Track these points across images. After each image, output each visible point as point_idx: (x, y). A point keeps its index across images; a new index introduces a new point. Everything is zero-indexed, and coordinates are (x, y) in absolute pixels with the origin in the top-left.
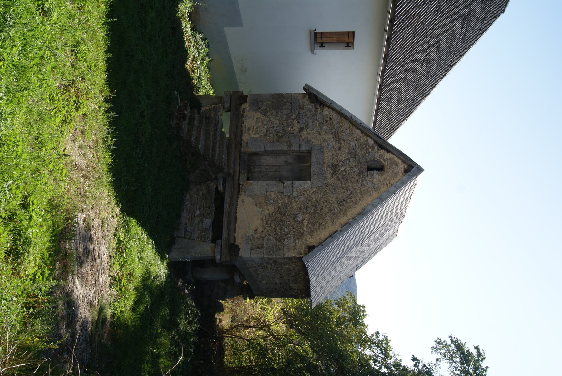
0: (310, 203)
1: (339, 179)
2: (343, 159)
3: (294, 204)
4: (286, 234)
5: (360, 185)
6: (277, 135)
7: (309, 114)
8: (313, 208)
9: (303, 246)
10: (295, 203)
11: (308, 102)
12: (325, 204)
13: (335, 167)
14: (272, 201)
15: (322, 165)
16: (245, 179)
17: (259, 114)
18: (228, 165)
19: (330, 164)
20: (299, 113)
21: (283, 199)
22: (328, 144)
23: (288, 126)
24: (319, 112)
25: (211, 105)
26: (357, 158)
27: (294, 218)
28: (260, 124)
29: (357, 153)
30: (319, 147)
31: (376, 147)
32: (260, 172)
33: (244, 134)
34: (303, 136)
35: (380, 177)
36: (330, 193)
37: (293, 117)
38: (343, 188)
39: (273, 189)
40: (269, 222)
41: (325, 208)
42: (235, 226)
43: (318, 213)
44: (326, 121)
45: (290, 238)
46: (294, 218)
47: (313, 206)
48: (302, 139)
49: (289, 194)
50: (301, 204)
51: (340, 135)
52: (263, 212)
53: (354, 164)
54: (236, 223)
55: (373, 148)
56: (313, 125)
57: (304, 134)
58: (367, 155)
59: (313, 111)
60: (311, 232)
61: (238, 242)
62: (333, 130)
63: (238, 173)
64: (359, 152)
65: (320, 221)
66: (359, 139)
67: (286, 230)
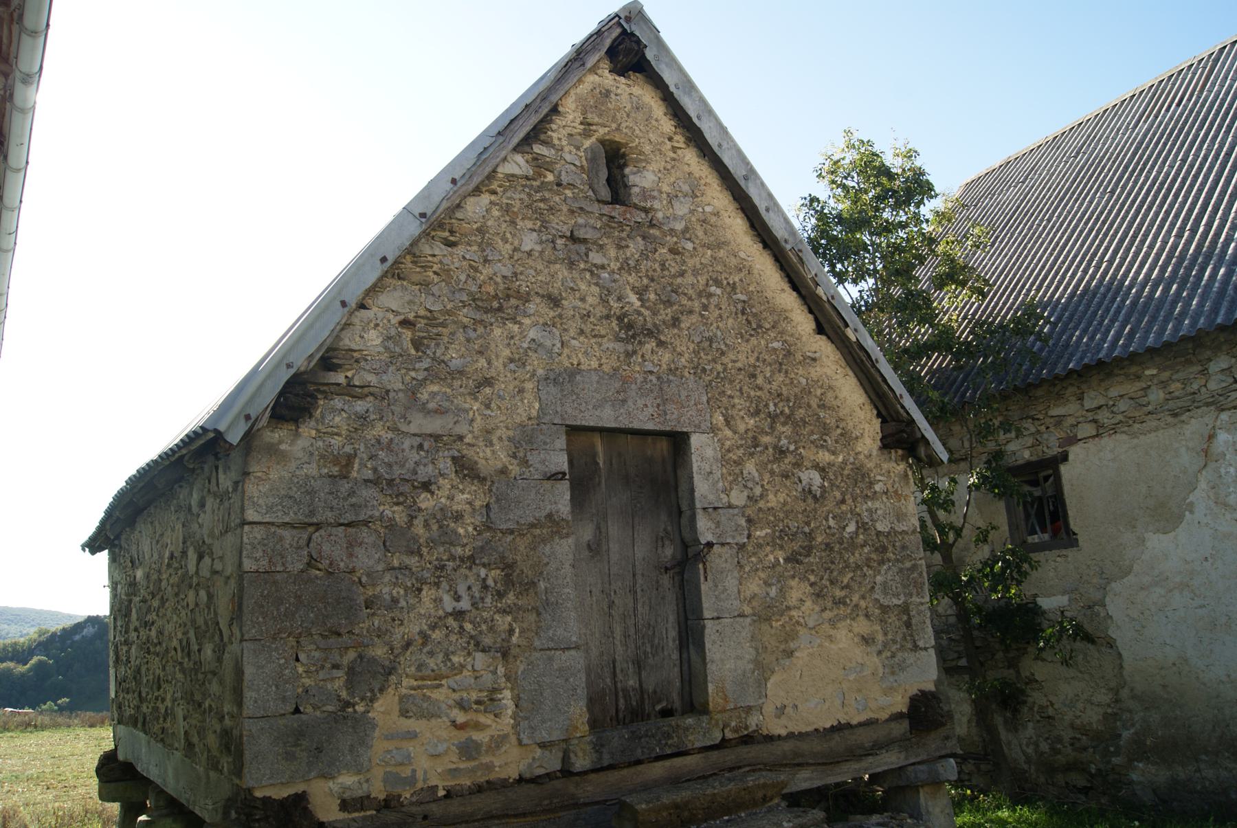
0: (766, 439)
1: (675, 322)
3: (773, 501)
4: (862, 526)
5: (689, 246)
6: (500, 595)
7: (379, 431)
9: (885, 466)
10: (771, 496)
11: (308, 430)
12: (760, 381)
14: (773, 592)
15: (625, 381)
16: (705, 718)
18: (765, 799)
19: (620, 347)
20: (375, 482)
21: (760, 546)
22: (536, 345)
24: (371, 378)
28: (436, 695)
29: (566, 230)
30: (553, 390)
31: (538, 149)
32: (639, 665)
33: (499, 774)
35: (653, 167)
36: (725, 360)
37: (399, 514)
38: (705, 307)
39: (726, 589)
40: (839, 593)
41: (775, 386)
42: (861, 725)
43: (792, 409)
44: (417, 344)
45: (869, 510)
46: (815, 497)
47: (772, 427)
48: (514, 469)
49: (743, 522)
50: (772, 473)
51: (491, 290)
52: (811, 624)
53: (612, 253)
54: (849, 726)
55: (540, 164)
57: (491, 457)
58: (569, 193)
59: (360, 406)
60: (847, 439)
61: (899, 703)
62: (465, 316)
63: (678, 762)
64: (561, 223)
65: (814, 403)
66: (507, 209)
67: (851, 528)
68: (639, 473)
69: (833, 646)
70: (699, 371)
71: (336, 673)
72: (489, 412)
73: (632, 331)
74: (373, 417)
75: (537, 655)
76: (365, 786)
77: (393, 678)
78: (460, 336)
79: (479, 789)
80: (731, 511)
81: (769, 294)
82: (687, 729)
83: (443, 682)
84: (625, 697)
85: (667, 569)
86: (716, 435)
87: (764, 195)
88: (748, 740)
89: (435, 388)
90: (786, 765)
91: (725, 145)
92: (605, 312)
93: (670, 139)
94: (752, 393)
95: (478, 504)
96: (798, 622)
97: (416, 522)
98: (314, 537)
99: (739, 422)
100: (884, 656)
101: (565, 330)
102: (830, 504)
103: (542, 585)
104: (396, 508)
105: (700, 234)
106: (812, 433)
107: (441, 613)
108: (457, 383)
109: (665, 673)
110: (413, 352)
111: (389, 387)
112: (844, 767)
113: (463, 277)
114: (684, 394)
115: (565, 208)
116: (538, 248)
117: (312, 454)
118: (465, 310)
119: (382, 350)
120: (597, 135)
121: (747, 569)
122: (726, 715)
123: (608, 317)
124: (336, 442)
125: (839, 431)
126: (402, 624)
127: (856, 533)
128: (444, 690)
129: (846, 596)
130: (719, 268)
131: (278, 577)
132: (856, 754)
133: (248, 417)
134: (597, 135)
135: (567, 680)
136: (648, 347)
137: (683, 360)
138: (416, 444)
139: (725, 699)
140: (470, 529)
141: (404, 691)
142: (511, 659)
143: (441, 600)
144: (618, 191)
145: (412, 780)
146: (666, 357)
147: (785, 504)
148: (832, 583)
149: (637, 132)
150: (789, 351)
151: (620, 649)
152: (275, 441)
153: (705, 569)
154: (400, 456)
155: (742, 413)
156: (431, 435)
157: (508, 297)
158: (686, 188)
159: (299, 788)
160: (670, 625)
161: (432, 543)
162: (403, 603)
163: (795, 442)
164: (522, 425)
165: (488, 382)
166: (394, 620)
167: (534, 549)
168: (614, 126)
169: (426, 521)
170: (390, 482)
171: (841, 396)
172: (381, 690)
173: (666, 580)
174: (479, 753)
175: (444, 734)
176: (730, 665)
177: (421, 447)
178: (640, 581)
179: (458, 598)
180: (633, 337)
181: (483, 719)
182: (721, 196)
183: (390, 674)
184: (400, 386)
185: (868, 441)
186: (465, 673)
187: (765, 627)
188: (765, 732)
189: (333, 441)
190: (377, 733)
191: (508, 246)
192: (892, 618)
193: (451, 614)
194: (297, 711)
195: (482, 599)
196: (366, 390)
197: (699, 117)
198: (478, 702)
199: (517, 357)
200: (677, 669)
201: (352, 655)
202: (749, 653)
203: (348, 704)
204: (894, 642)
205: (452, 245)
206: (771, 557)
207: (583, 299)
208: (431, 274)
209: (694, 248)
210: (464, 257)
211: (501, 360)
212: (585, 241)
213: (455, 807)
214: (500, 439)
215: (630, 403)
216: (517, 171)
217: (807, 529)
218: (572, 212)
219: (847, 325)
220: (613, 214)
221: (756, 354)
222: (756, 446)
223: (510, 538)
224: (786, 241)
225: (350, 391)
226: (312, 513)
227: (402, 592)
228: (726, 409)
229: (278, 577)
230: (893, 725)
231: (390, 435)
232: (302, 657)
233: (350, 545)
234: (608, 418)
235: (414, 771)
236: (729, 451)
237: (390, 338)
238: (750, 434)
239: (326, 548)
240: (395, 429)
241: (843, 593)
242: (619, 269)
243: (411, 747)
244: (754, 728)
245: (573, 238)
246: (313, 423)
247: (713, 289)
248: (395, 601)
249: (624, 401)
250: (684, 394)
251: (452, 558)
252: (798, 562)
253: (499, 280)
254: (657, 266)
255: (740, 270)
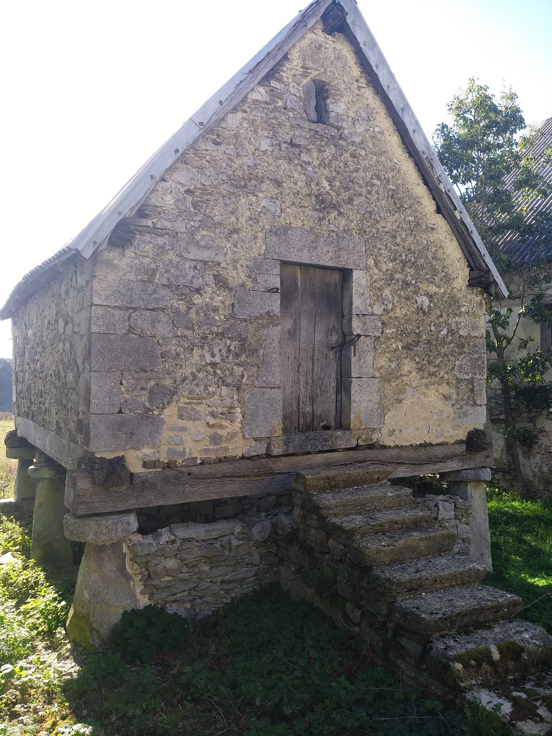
0: (398, 276)
2: (303, 177)
3: (399, 313)
4: (451, 332)
5: (363, 153)
6: (237, 355)
7: (171, 256)
8: (407, 269)
9: (469, 297)
10: (398, 310)
11: (130, 253)
12: (398, 240)
13: (324, 205)
14: (393, 365)
16: (348, 432)
17: (169, 414)
18: (378, 479)
19: (315, 214)
20: (168, 286)
21: (388, 339)
23: (211, 322)
24: (168, 224)
25: (129, 578)
26: (302, 142)
27: (424, 313)
28: (198, 408)
30: (274, 238)
31: (273, 83)
32: (313, 400)
34: (243, 277)
36: (378, 226)
37: (182, 306)
38: (369, 192)
39: (365, 362)
40: (432, 369)
42: (437, 444)
44: (195, 205)
45: (457, 323)
46: (424, 313)
47: (403, 269)
48: (249, 284)
49: (379, 324)
50: (400, 296)
51: (240, 174)
53: (315, 154)
54: (431, 445)
56: (207, 247)
57: (237, 276)
58: (291, 114)
59: (160, 241)
60: (448, 279)
61: (462, 435)
62: (225, 189)
63: (330, 455)
64: (285, 134)
65: (430, 255)
66: (252, 123)
67: (444, 332)
68: (321, 291)
69: (425, 399)
70: (362, 231)
71: (143, 392)
72: (236, 249)
73: (324, 205)
74: (168, 247)
75: (257, 390)
76: (157, 455)
77: (175, 397)
78: (221, 201)
79: (220, 461)
80: (373, 317)
81: (409, 187)
82: (337, 437)
83: (203, 401)
84: (303, 417)
85: (332, 348)
86: (368, 272)
87: (413, 121)
88: (371, 447)
89: (205, 233)
90: (392, 463)
91: (392, 87)
92: (308, 192)
93: (357, 81)
94: (393, 247)
95: (227, 303)
96: (406, 384)
97: (191, 311)
98: (132, 315)
99: (383, 265)
100: (455, 407)
101: (283, 202)
102: (433, 317)
103: (261, 352)
104: (180, 302)
105: (370, 145)
106: (427, 274)
107: (204, 363)
108: (218, 231)
109: (327, 406)
110: (192, 210)
111: (178, 230)
112: (426, 467)
113: (224, 165)
114: (352, 245)
115: (288, 124)
116: (270, 149)
117: (132, 267)
118: (224, 186)
119: (174, 207)
120: (311, 76)
121: (379, 352)
122: (360, 432)
123: (310, 195)
124: (146, 261)
125: (443, 274)
126: (181, 368)
127: (447, 335)
128: (203, 406)
129: (437, 371)
130: (380, 168)
131: (112, 337)
132: (432, 461)
133: (95, 243)
134: (311, 76)
135: (272, 405)
136: (332, 215)
137: (353, 225)
138: (192, 266)
139: (360, 422)
140: (222, 317)
141: (181, 405)
142: (242, 391)
143: (204, 356)
144: (321, 114)
145: (183, 453)
146: (343, 222)
147: (406, 315)
148: (429, 363)
149: (337, 75)
150: (418, 223)
151: (302, 390)
152: (111, 258)
153: (355, 349)
154: (183, 272)
155: (385, 259)
156: (201, 261)
157: (250, 179)
158: (364, 115)
159: (120, 454)
160: (331, 380)
161: (200, 324)
162: (182, 356)
163: (416, 279)
164: (255, 259)
165: (236, 231)
166: (177, 365)
167: (258, 331)
168: (322, 70)
169: (197, 311)
170: (177, 287)
171: (447, 252)
172: (168, 404)
173: (331, 354)
174: (221, 441)
175: (202, 430)
176: (364, 404)
177: (195, 267)
178: (316, 353)
179: (213, 356)
180: (324, 208)
181: (224, 423)
182: (385, 121)
183: (174, 395)
184: (183, 230)
185: (460, 281)
186: (216, 397)
187: (387, 385)
188: (382, 443)
189: (144, 261)
190: (165, 427)
191: (252, 147)
192: (463, 386)
193: (209, 364)
194: (120, 412)
195: (227, 357)
196: (164, 231)
197: (377, 66)
198: (222, 414)
199: (254, 216)
200: (334, 404)
201: (152, 383)
202: (376, 398)
203: (149, 410)
204: (463, 400)
205: (217, 144)
206: (394, 346)
207: (295, 183)
208: (205, 162)
209: (366, 154)
210: (225, 152)
211: (244, 218)
212: (299, 146)
213: (206, 470)
214: (242, 266)
215: (319, 249)
216: (260, 98)
217: (417, 331)
218: (292, 127)
219: (455, 209)
220: (317, 129)
221: (398, 224)
222: (393, 280)
223: (244, 324)
224: (423, 153)
225: (155, 231)
226: (131, 302)
227: (182, 350)
228: (376, 256)
229: (112, 337)
230: (456, 446)
231: (178, 259)
232: (124, 382)
233: (153, 322)
234: (305, 258)
235: (184, 448)
236: (375, 282)
237: (179, 200)
238: (389, 272)
239: (139, 322)
240: (180, 256)
241: (435, 369)
242: (318, 165)
243: (182, 435)
244: (376, 440)
245: (292, 144)
246: (133, 249)
247: (375, 181)
248: (178, 355)
249: (316, 248)
250: (352, 245)
251: (211, 333)
252: (410, 349)
253: (245, 168)
254: (342, 164)
255: (393, 170)
